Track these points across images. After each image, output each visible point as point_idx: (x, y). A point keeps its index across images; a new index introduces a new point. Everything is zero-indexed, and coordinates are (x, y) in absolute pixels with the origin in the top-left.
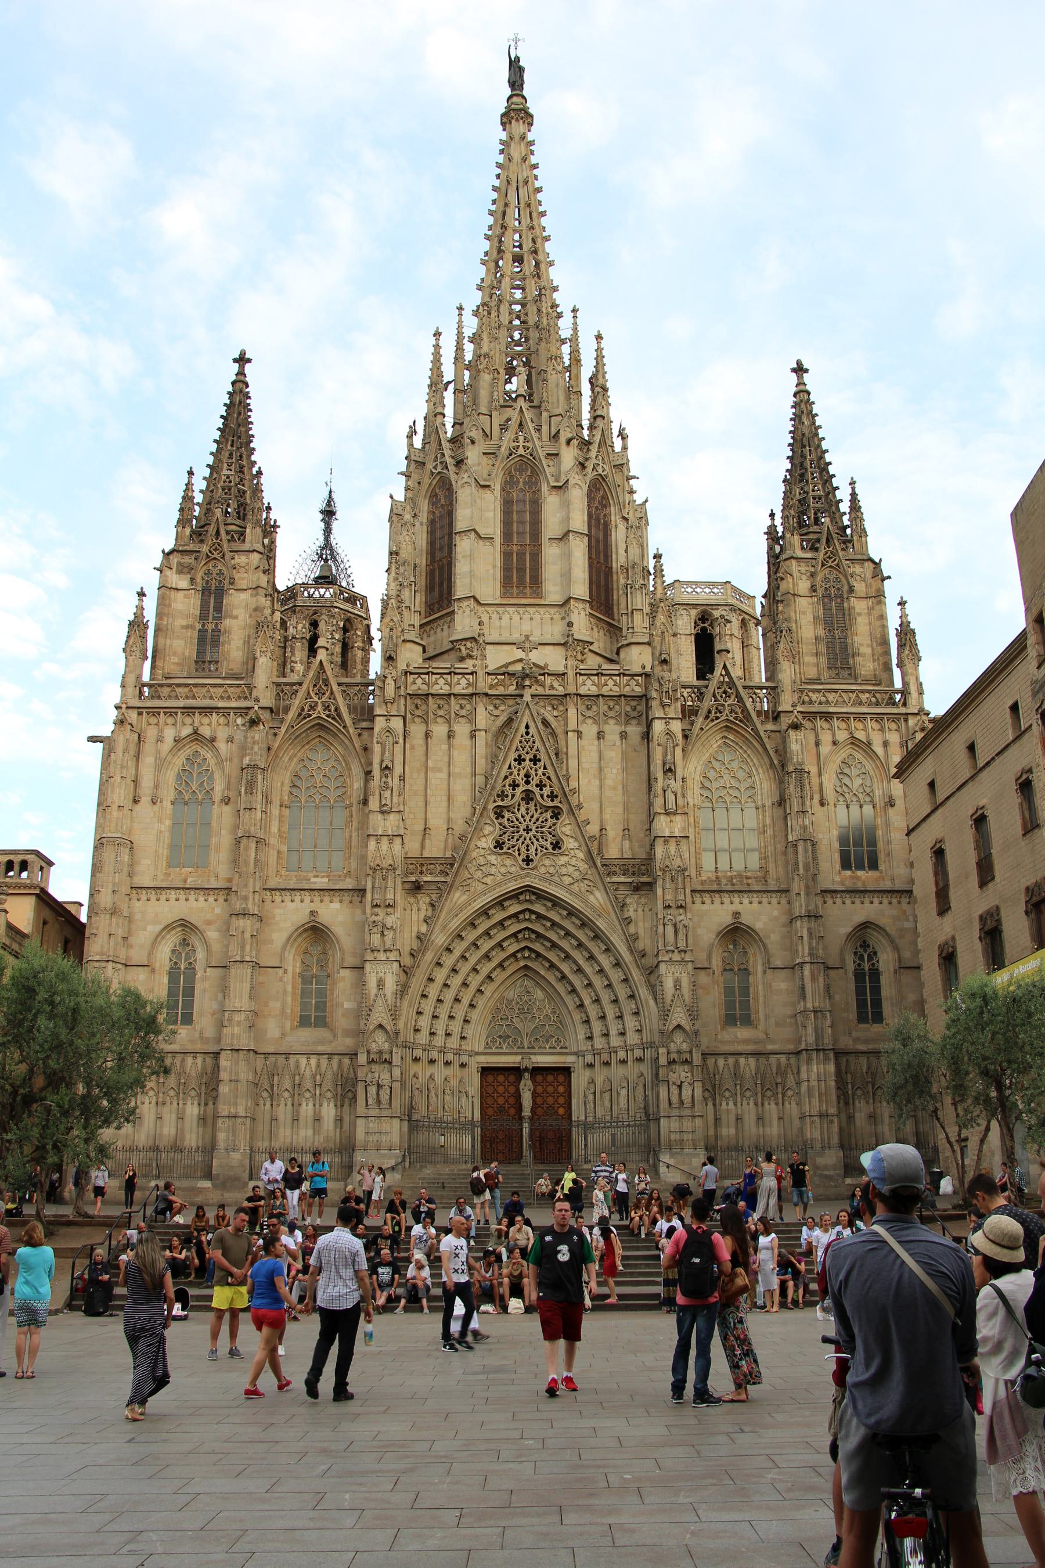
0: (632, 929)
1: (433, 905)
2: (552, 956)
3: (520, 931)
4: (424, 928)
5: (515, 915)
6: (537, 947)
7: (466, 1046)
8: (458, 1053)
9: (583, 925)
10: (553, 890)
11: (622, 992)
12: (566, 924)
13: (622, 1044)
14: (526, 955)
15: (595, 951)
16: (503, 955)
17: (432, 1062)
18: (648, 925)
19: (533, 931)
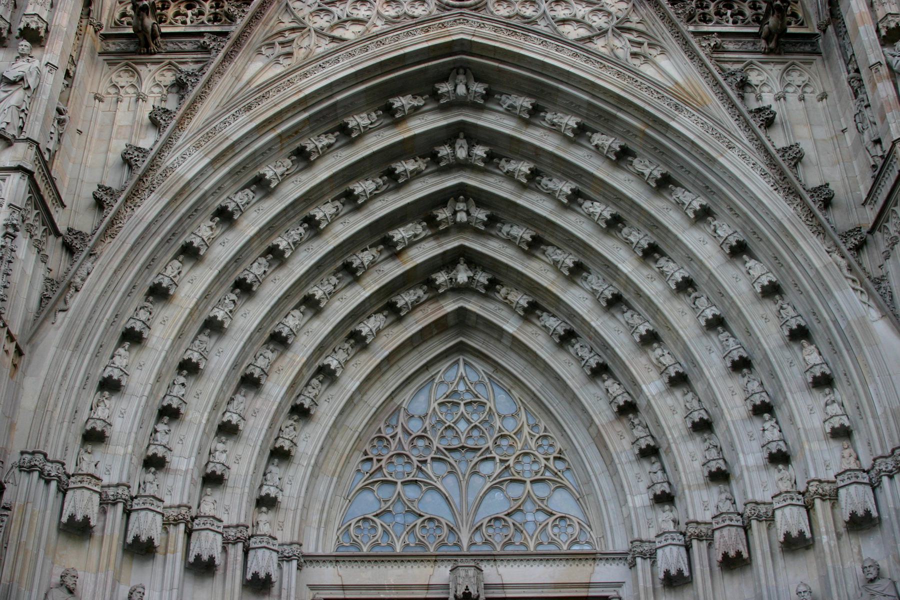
0: (778, 139)
1: (180, 86)
2: (537, 270)
3: (440, 199)
4: (148, 140)
5: (425, 148)
6: (492, 248)
7: (279, 527)
8: (244, 541)
9: (623, 157)
10: (532, 49)
11: (766, 327)
12: (579, 157)
13: (785, 486)
14: (462, 276)
15: (672, 220)
16: (392, 270)
17: (141, 550)
18: (822, 133)
19: (481, 199)
